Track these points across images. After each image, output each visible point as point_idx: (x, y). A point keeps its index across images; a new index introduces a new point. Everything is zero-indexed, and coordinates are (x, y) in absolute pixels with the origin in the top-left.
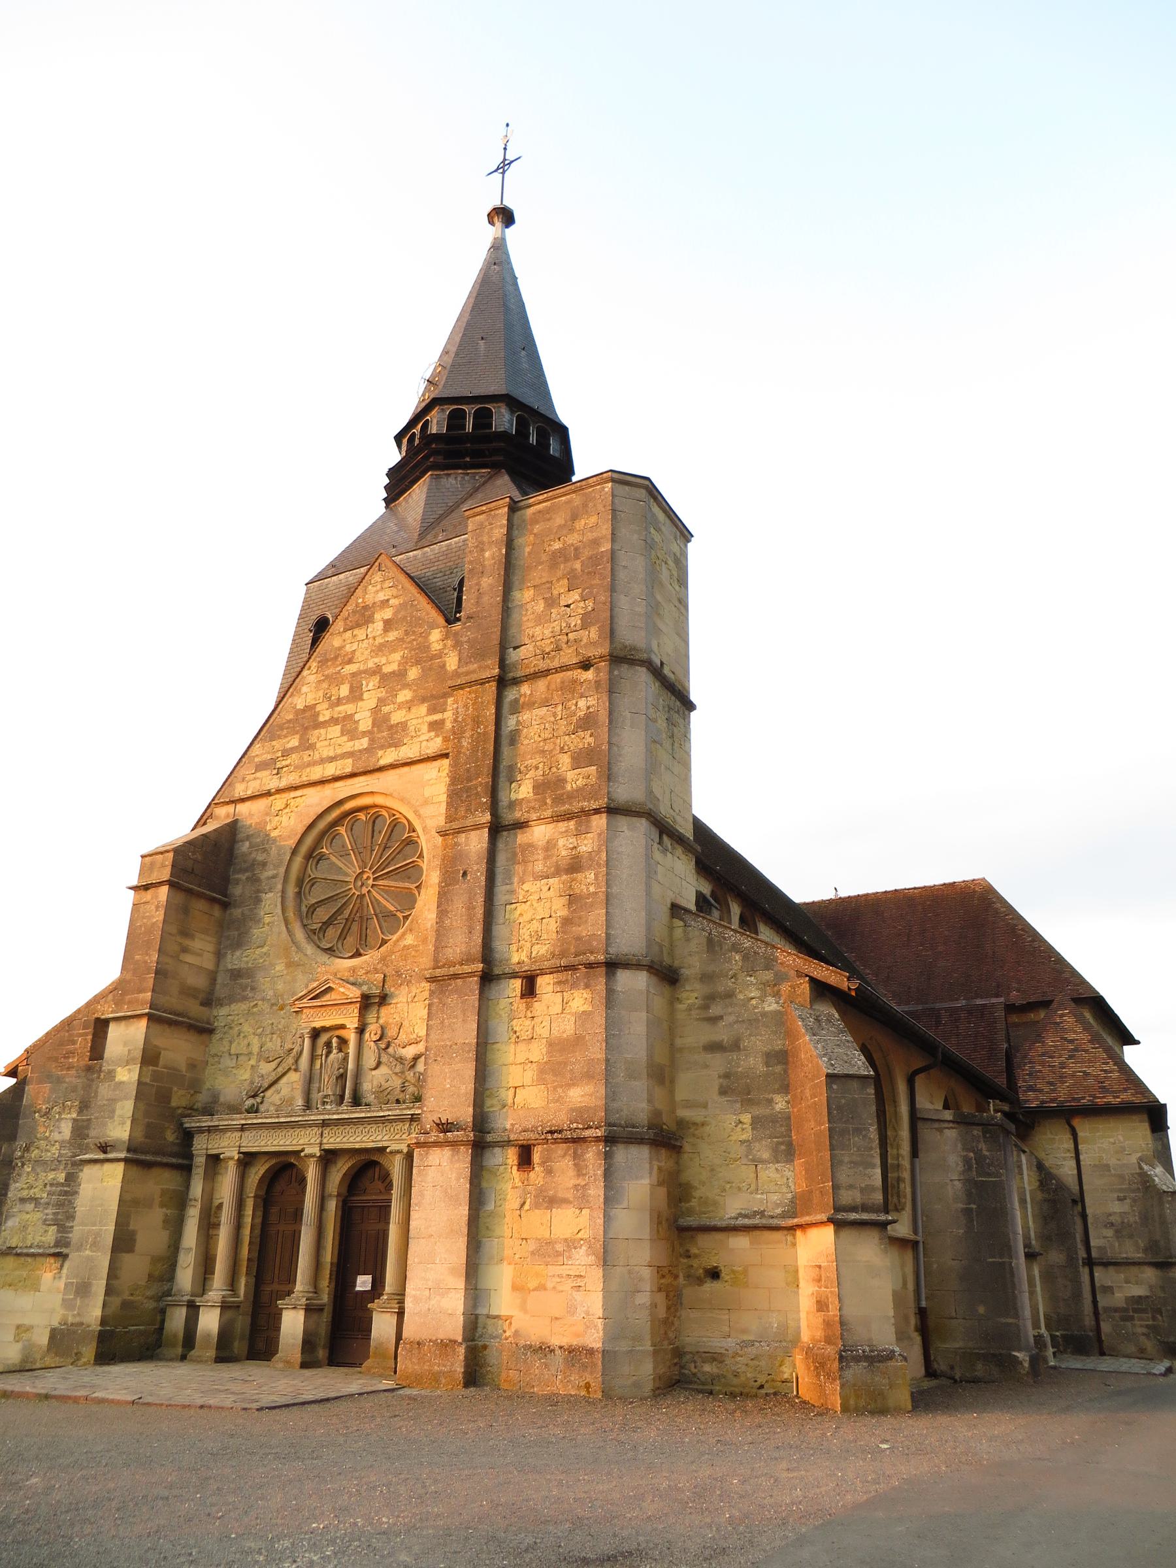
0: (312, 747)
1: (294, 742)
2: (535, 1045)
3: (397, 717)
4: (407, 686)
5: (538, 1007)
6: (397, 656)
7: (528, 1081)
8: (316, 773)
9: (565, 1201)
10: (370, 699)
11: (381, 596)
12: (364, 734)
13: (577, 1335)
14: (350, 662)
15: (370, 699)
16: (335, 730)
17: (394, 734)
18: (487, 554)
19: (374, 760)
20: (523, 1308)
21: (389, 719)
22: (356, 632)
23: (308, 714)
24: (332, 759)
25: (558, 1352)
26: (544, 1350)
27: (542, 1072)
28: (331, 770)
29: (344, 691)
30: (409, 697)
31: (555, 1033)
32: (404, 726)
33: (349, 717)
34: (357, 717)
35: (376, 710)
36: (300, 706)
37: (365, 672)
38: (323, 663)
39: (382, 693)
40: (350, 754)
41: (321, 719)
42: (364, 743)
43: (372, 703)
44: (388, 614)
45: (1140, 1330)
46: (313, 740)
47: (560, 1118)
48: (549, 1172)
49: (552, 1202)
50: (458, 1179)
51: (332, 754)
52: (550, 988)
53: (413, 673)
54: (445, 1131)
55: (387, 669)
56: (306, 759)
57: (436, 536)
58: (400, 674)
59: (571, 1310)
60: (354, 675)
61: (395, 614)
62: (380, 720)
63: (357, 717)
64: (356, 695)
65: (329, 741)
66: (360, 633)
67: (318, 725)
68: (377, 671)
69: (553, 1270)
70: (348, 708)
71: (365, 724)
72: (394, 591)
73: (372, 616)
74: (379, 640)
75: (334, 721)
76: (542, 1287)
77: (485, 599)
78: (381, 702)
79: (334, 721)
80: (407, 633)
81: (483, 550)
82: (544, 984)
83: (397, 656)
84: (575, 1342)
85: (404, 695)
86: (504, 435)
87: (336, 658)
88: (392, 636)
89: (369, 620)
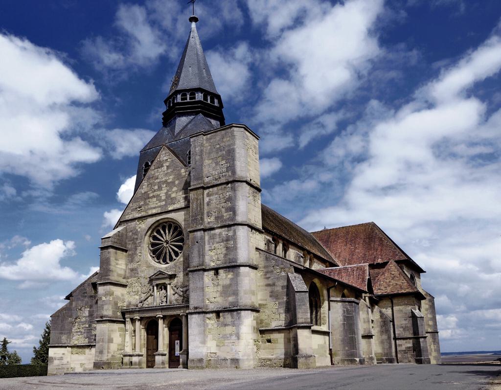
0: (148, 204)
1: (142, 203)
2: (219, 287)
3: (173, 195)
4: (175, 186)
5: (219, 277)
6: (171, 177)
7: (218, 296)
8: (150, 212)
9: (229, 325)
10: (164, 190)
11: (165, 158)
12: (163, 200)
13: (233, 356)
14: (157, 179)
15: (164, 190)
16: (155, 199)
17: (173, 201)
18: (197, 149)
19: (167, 208)
20: (219, 350)
21: (170, 196)
22: (158, 169)
23: (145, 195)
24: (154, 208)
25: (229, 360)
26: (225, 360)
27: (221, 293)
28: (154, 211)
29: (156, 187)
30: (176, 189)
31: (224, 283)
32: (175, 198)
33: (158, 196)
34: (161, 195)
35: (166, 193)
36: (143, 192)
37: (162, 182)
38: (149, 178)
39: (168, 188)
40: (160, 206)
41: (150, 196)
42: (164, 203)
43: (165, 191)
44: (167, 164)
45: (409, 356)
46: (148, 202)
47: (227, 305)
48: (224, 318)
49: (226, 325)
50: (200, 321)
51: (154, 206)
52: (222, 272)
53: (177, 182)
54: (196, 309)
55: (169, 181)
56: (146, 208)
57: (180, 137)
58: (173, 182)
59: (232, 350)
60: (159, 183)
61: (170, 164)
62: (168, 196)
63: (161, 195)
64: (160, 189)
65: (153, 202)
66: (160, 170)
67: (149, 198)
68: (166, 182)
69: (226, 341)
70: (158, 193)
71: (163, 198)
72: (169, 157)
73: (162, 165)
74: (166, 172)
75: (154, 196)
76: (224, 345)
77: (197, 163)
78: (168, 191)
79: (154, 196)
80: (174, 170)
81: (195, 148)
82: (221, 271)
83: (171, 177)
84: (233, 357)
85: (175, 189)
86: (200, 102)
87: (153, 177)
88: (170, 171)
89: (162, 166)
